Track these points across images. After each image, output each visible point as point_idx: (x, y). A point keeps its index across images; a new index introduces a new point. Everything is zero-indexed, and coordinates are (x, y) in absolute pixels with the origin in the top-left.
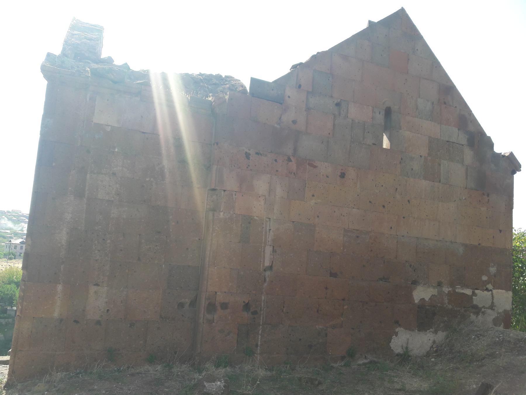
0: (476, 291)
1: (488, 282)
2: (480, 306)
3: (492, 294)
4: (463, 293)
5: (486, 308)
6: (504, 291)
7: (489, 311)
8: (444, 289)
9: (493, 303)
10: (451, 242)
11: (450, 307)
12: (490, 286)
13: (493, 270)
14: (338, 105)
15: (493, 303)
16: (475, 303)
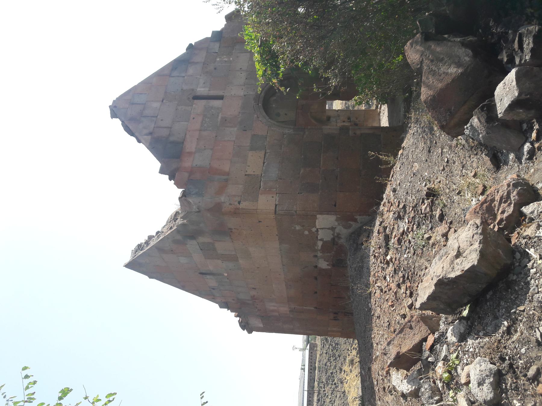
0: (319, 238)
1: (310, 231)
2: (332, 236)
3: (320, 229)
4: (322, 246)
5: (334, 233)
6: (317, 221)
7: (337, 230)
8: (318, 255)
9: (329, 229)
10: (281, 250)
11: (333, 252)
12: (314, 230)
13: (298, 228)
14: (213, 289)
15: (329, 229)
16: (330, 239)
